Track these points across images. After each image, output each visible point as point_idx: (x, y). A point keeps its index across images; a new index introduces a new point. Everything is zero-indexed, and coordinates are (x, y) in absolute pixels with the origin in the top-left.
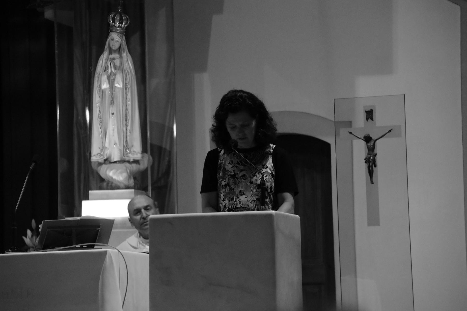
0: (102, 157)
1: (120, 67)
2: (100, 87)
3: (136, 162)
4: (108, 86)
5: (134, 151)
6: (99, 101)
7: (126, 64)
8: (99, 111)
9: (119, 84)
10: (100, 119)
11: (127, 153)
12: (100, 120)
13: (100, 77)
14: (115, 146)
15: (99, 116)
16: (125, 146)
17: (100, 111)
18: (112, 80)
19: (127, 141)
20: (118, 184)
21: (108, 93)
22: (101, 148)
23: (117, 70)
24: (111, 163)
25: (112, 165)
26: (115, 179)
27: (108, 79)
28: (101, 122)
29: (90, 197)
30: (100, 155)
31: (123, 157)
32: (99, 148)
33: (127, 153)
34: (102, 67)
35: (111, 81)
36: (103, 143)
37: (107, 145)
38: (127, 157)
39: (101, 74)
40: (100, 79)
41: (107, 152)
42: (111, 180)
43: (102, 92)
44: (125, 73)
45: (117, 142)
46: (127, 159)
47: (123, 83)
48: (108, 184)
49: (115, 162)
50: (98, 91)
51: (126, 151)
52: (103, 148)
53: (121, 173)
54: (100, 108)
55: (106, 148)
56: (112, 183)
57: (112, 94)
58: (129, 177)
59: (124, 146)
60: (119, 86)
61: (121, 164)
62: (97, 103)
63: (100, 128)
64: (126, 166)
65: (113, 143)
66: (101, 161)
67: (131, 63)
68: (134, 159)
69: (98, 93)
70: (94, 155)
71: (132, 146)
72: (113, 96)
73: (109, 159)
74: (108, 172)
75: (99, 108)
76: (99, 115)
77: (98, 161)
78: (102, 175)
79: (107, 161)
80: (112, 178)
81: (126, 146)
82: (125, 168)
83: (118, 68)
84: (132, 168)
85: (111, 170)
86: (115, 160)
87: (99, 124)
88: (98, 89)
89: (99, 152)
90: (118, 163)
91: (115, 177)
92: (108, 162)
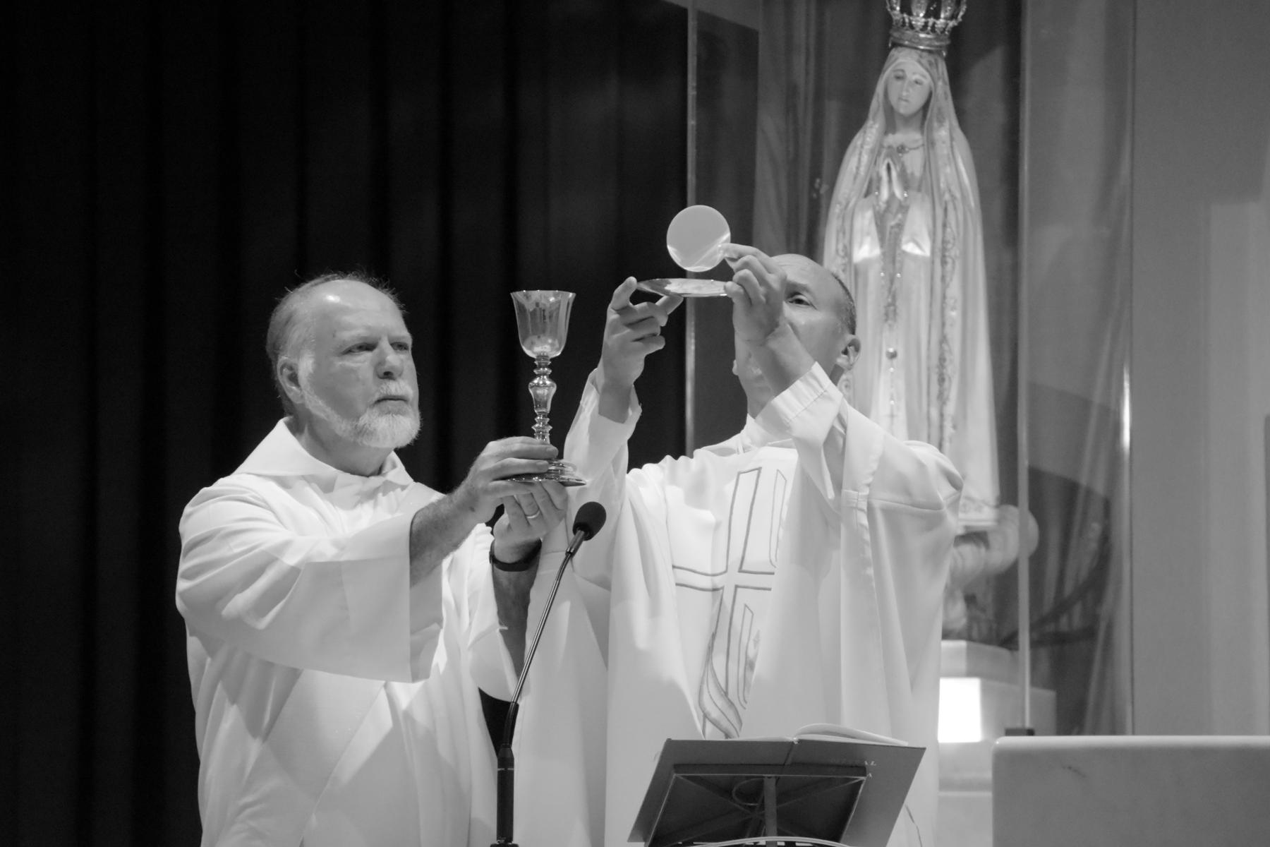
1: (922, 179)
2: (848, 254)
4: (877, 251)
7: (948, 170)
18: (892, 227)
28: (846, 386)
34: (858, 181)
35: (890, 233)
57: (892, 281)
60: (917, 251)
67: (964, 164)
72: (893, 289)
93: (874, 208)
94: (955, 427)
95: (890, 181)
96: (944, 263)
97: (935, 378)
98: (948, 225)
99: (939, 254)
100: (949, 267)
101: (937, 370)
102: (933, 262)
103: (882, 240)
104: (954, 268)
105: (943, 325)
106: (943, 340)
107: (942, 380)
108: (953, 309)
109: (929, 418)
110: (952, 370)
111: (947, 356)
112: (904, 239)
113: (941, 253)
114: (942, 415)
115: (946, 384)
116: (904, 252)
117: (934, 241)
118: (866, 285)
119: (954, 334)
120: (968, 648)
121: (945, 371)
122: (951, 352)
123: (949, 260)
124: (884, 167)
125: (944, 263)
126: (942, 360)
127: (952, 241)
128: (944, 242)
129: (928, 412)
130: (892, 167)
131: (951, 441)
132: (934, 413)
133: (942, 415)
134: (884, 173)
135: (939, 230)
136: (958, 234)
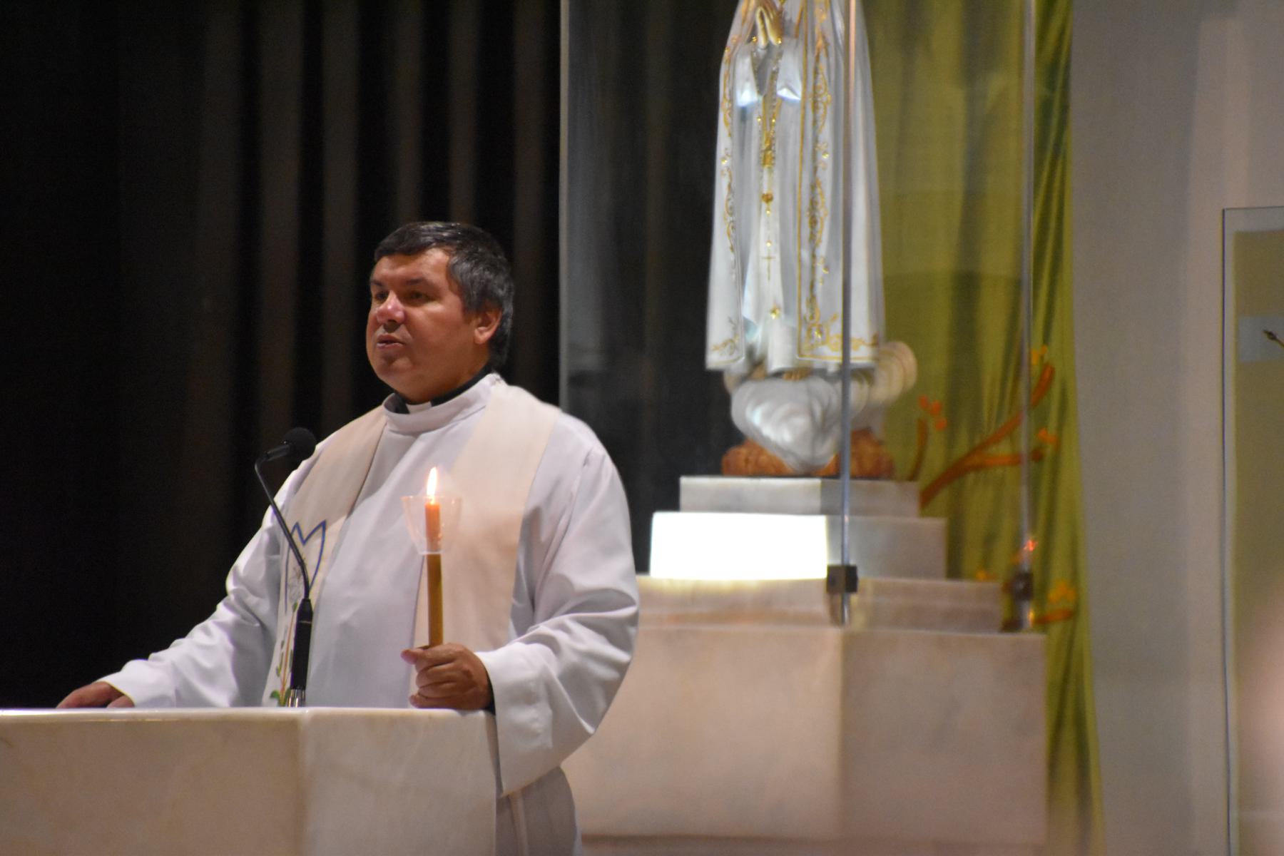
6: (729, 151)
8: (730, 186)
10: (731, 214)
12: (731, 219)
13: (732, 62)
15: (730, 204)
17: (732, 185)
19: (812, 298)
20: (779, 455)
21: (757, 120)
23: (787, 40)
26: (767, 440)
28: (733, 228)
29: (684, 499)
31: (798, 358)
37: (747, 312)
38: (813, 356)
40: (731, 72)
41: (756, 337)
44: (813, 49)
46: (817, 364)
49: (778, 374)
50: (727, 115)
51: (811, 337)
54: (731, 177)
56: (761, 451)
58: (821, 428)
59: (802, 320)
61: (795, 379)
64: (810, 392)
75: (727, 174)
76: (729, 200)
79: (756, 363)
80: (758, 431)
81: (812, 317)
83: (793, 31)
87: (729, 235)
90: (785, 376)
91: (769, 431)
93: (752, 53)
94: (827, 268)
95: (765, 29)
96: (815, 108)
97: (806, 221)
98: (820, 71)
99: (810, 100)
100: (821, 112)
101: (808, 213)
102: (804, 108)
104: (825, 112)
105: (815, 170)
106: (814, 186)
107: (813, 222)
108: (825, 153)
109: (800, 261)
110: (824, 212)
111: (819, 199)
112: (779, 85)
113: (812, 98)
114: (813, 256)
115: (819, 226)
116: (783, 99)
117: (805, 87)
118: (751, 128)
119: (826, 176)
120: (823, 483)
121: (817, 214)
122: (822, 194)
123: (821, 105)
124: (758, 15)
125: (815, 108)
126: (813, 204)
127: (823, 86)
128: (815, 87)
129: (800, 254)
130: (765, 14)
131: (823, 282)
132: (806, 255)
133: (813, 256)
134: (759, 22)
135: (810, 75)
136: (830, 81)
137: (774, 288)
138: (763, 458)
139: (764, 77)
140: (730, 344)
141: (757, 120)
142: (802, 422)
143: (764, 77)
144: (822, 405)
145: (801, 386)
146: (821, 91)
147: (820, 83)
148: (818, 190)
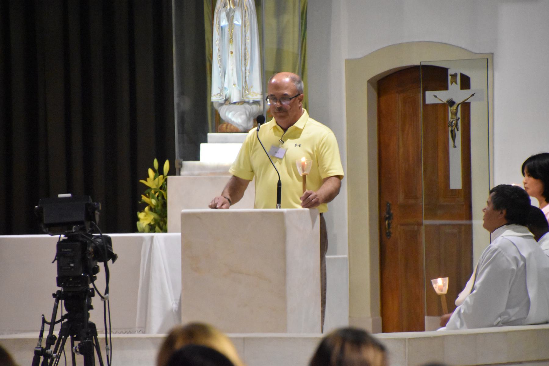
0: (221, 97)
2: (219, 24)
3: (256, 102)
5: (254, 92)
9: (238, 21)
10: (219, 57)
11: (246, 94)
13: (219, 13)
14: (233, 86)
15: (219, 54)
16: (244, 87)
18: (231, 16)
19: (246, 81)
20: (237, 126)
21: (227, 30)
22: (221, 87)
23: (236, 7)
24: (230, 103)
25: (232, 106)
26: (233, 122)
27: (227, 16)
30: (219, 96)
31: (242, 98)
32: (219, 88)
33: (246, 94)
34: (222, 2)
36: (222, 83)
37: (226, 85)
38: (246, 98)
39: (220, 9)
41: (227, 92)
42: (230, 123)
43: (222, 29)
45: (236, 82)
46: (247, 100)
47: (242, 19)
48: (227, 126)
49: (235, 103)
51: (245, 92)
52: (222, 89)
53: (241, 115)
55: (225, 88)
56: (231, 125)
58: (249, 119)
59: (243, 88)
61: (240, 105)
62: (216, 41)
63: (220, 67)
64: (245, 108)
65: (232, 83)
66: (222, 101)
68: (253, 100)
69: (217, 30)
70: (214, 95)
71: (252, 87)
73: (229, 99)
74: (227, 114)
76: (218, 53)
77: (218, 102)
78: (222, 115)
79: (227, 101)
80: (231, 120)
81: (246, 87)
82: (244, 110)
83: (237, 4)
84: (252, 110)
85: (230, 112)
86: (234, 101)
88: (217, 26)
89: (219, 92)
90: (237, 104)
91: (233, 119)
92: (228, 103)
103: (228, 20)
118: (225, 33)
135: (243, 17)
137: (234, 79)
138: (232, 127)
139: (230, 18)
140: (220, 94)
141: (227, 30)
142: (244, 117)
143: (230, 18)
144: (248, 111)
145: (242, 106)
146: (247, 22)
147: (246, 19)
148: (246, 50)
